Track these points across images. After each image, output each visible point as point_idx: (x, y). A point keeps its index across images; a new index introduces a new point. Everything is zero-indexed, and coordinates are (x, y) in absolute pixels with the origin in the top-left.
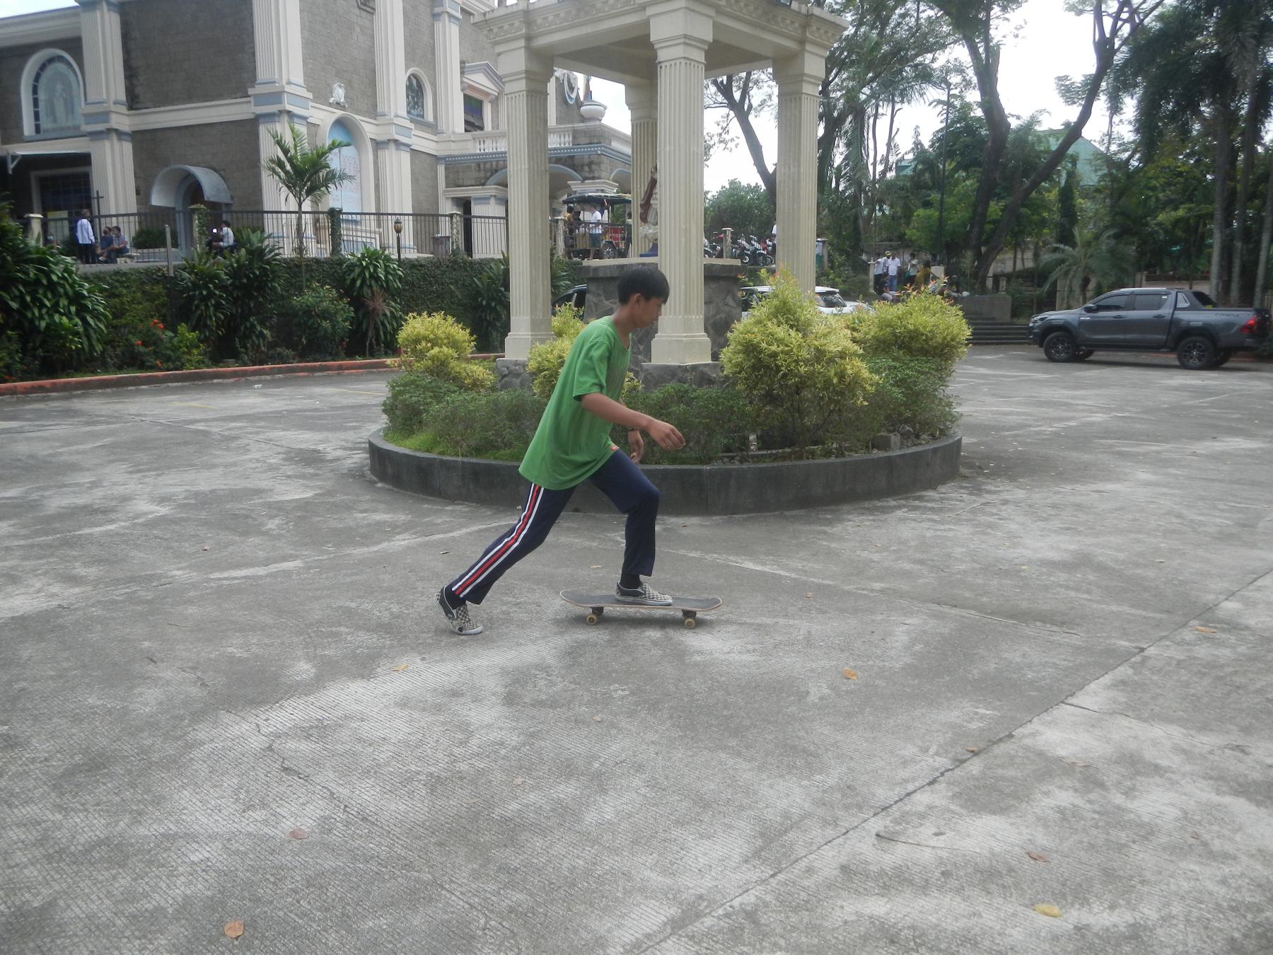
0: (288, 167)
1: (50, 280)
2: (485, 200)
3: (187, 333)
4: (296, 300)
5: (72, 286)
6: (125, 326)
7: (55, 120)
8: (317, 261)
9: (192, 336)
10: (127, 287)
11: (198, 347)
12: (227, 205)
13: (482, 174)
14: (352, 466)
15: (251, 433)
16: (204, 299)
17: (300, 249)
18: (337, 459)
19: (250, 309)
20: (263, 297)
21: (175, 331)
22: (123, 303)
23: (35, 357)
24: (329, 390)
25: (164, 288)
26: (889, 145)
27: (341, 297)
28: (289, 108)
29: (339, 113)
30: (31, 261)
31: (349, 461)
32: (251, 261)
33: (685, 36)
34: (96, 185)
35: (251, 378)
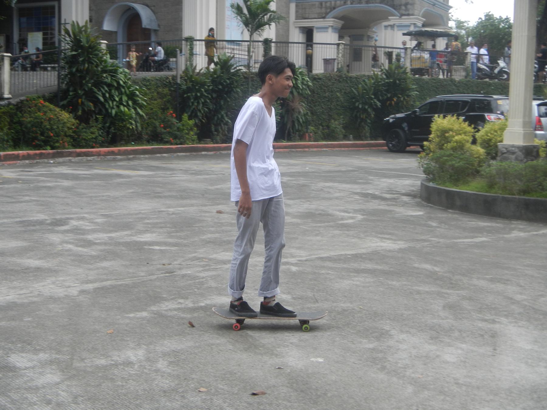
1: (118, 83)
2: (324, 29)
3: (188, 121)
9: (191, 122)
11: (191, 129)
12: (155, 31)
13: (323, 10)
16: (196, 98)
17: (248, 66)
21: (180, 119)
25: (170, 90)
35: (223, 152)
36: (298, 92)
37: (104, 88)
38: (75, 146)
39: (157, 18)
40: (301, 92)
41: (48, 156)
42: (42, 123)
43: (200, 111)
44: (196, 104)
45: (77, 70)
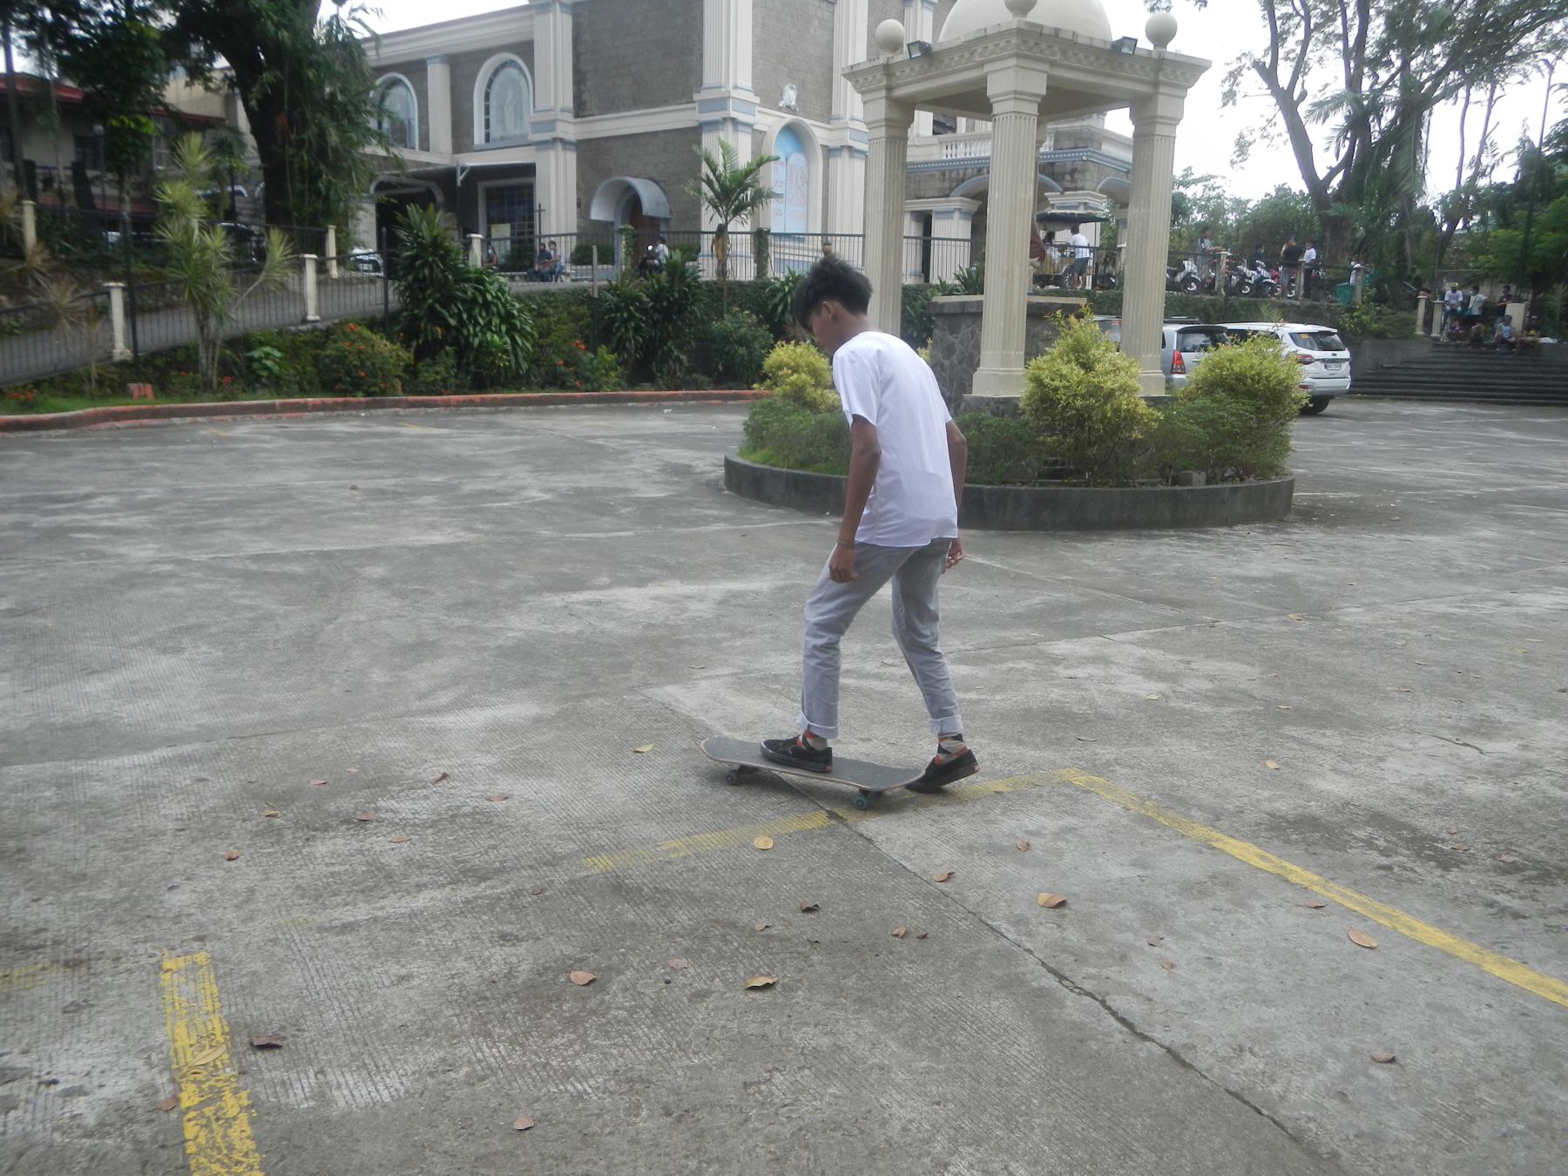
0: (717, 186)
2: (948, 214)
4: (715, 325)
5: (504, 305)
6: (550, 345)
8: (740, 284)
9: (611, 358)
10: (555, 307)
11: (616, 370)
12: (666, 220)
13: (947, 184)
16: (625, 322)
17: (722, 272)
18: (704, 473)
19: (669, 333)
20: (683, 321)
21: (595, 352)
23: (468, 373)
25: (589, 308)
26: (1483, 143)
27: (760, 322)
28: (734, 114)
29: (789, 118)
30: (469, 280)
32: (672, 282)
33: (1015, 92)
35: (665, 403)
38: (412, 393)
41: (357, 407)
42: (346, 357)
45: (416, 279)
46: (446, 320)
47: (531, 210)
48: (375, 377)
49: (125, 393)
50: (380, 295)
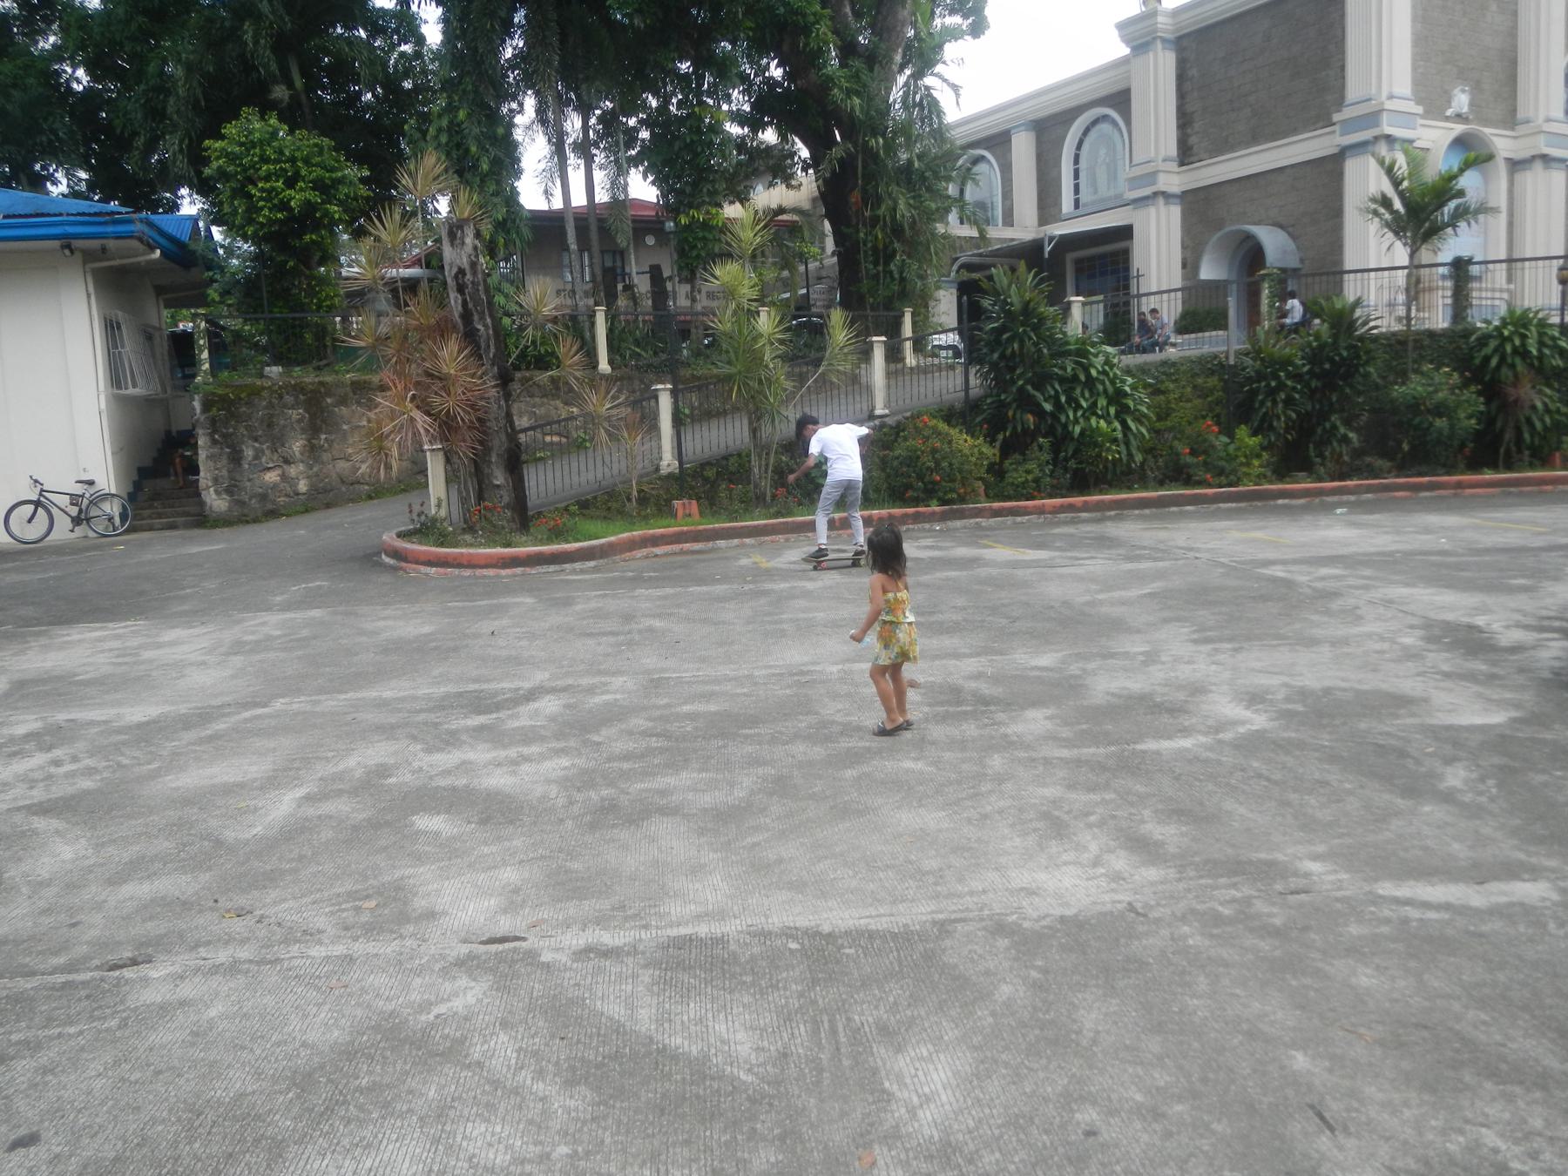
1: (1088, 375)
3: (1245, 436)
4: (1398, 391)
5: (1113, 382)
6: (1170, 429)
7: (1096, 192)
8: (1431, 334)
9: (1253, 441)
11: (1258, 456)
12: (1295, 270)
14: (1557, 664)
15: (1357, 588)
16: (1272, 393)
18: (1516, 649)
19: (1331, 404)
20: (1351, 386)
21: (1231, 435)
22: (1169, 402)
23: (1066, 469)
24: (1451, 520)
25: (1221, 380)
27: (1465, 384)
28: (1388, 130)
29: (1459, 128)
30: (1068, 353)
31: (1545, 654)
32: (1335, 337)
34: (1137, 261)
36: (1532, 365)
37: (1054, 388)
39: (1298, 248)
40: (1536, 363)
41: (931, 518)
43: (1278, 418)
44: (1269, 404)
45: (1002, 356)
46: (1039, 405)
47: (1127, 278)
48: (953, 480)
49: (673, 514)
50: (960, 380)
